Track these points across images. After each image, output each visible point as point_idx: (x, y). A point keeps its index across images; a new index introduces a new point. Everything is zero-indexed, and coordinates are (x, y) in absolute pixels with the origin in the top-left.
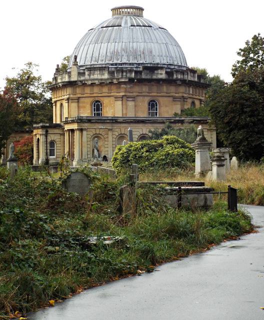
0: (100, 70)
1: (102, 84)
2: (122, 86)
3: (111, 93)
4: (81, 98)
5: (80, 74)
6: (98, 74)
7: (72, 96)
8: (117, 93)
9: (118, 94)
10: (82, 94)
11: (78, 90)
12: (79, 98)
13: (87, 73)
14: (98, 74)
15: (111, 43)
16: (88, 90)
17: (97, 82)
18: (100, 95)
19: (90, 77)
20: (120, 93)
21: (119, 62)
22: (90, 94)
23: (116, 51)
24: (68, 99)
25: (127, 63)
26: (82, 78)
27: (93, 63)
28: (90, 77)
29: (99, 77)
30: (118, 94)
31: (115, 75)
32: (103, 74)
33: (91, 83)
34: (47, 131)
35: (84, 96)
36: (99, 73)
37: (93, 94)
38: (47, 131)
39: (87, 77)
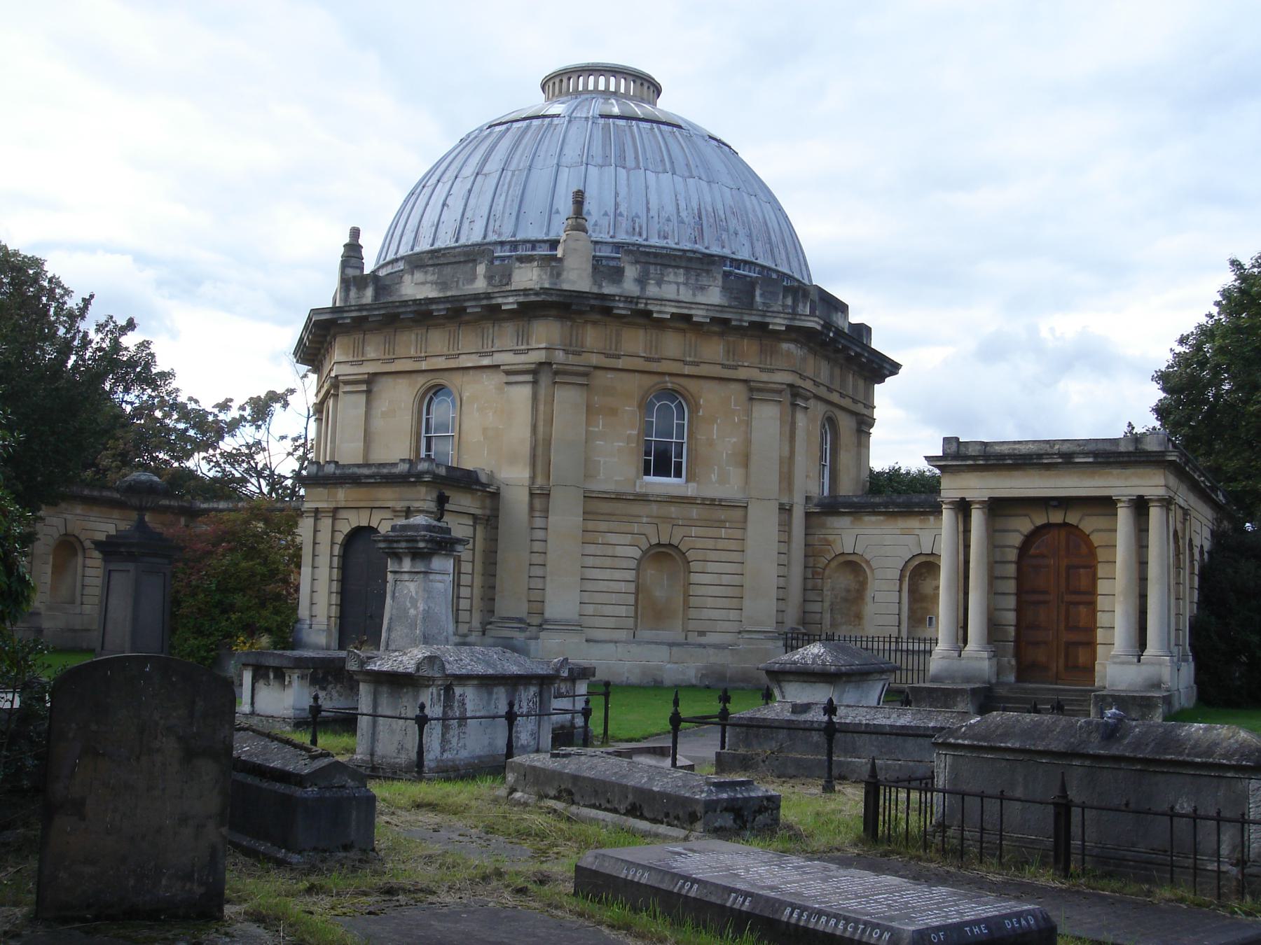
0: (687, 269)
1: (721, 326)
2: (785, 346)
3: (735, 368)
4: (599, 373)
5: (604, 268)
6: (678, 284)
7: (560, 356)
8: (762, 370)
9: (765, 377)
10: (608, 356)
11: (592, 337)
12: (596, 368)
13: (631, 272)
14: (678, 284)
15: (684, 178)
16: (635, 342)
17: (699, 315)
18: (687, 370)
19: (643, 289)
20: (772, 371)
21: (726, 252)
22: (648, 359)
23: (710, 209)
24: (536, 371)
25: (752, 263)
26: (608, 289)
27: (622, 237)
28: (643, 289)
29: (685, 295)
30: (765, 377)
31: (758, 299)
32: (702, 288)
33: (672, 314)
34: (442, 500)
35: (620, 363)
36: (681, 279)
37: (659, 360)
38: (442, 500)
39: (629, 286)
